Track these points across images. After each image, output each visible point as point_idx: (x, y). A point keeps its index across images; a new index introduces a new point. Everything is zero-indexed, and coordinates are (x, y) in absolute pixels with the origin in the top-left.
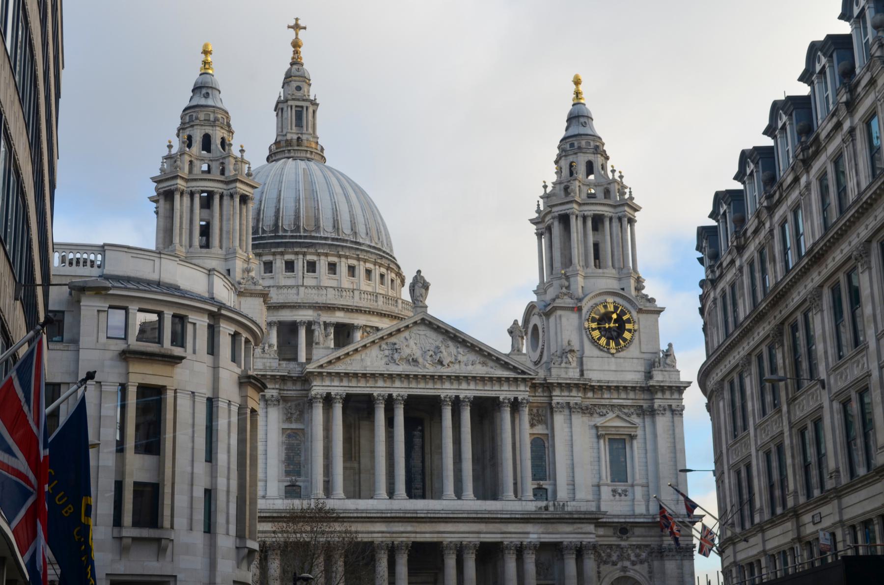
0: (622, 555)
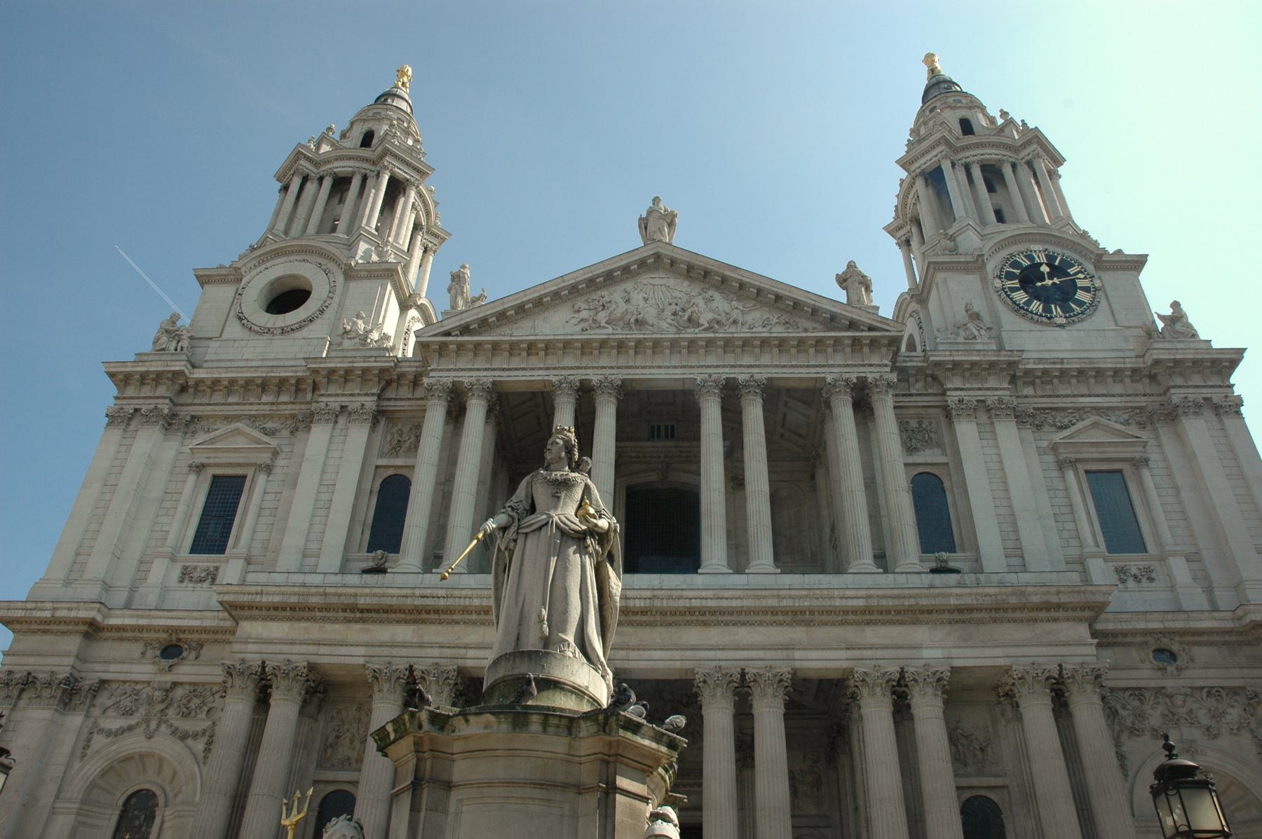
0: (1171, 712)
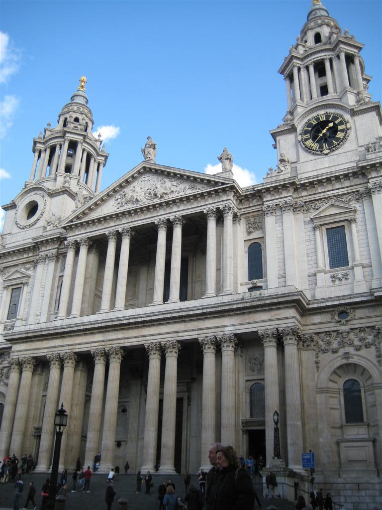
0: (343, 342)
